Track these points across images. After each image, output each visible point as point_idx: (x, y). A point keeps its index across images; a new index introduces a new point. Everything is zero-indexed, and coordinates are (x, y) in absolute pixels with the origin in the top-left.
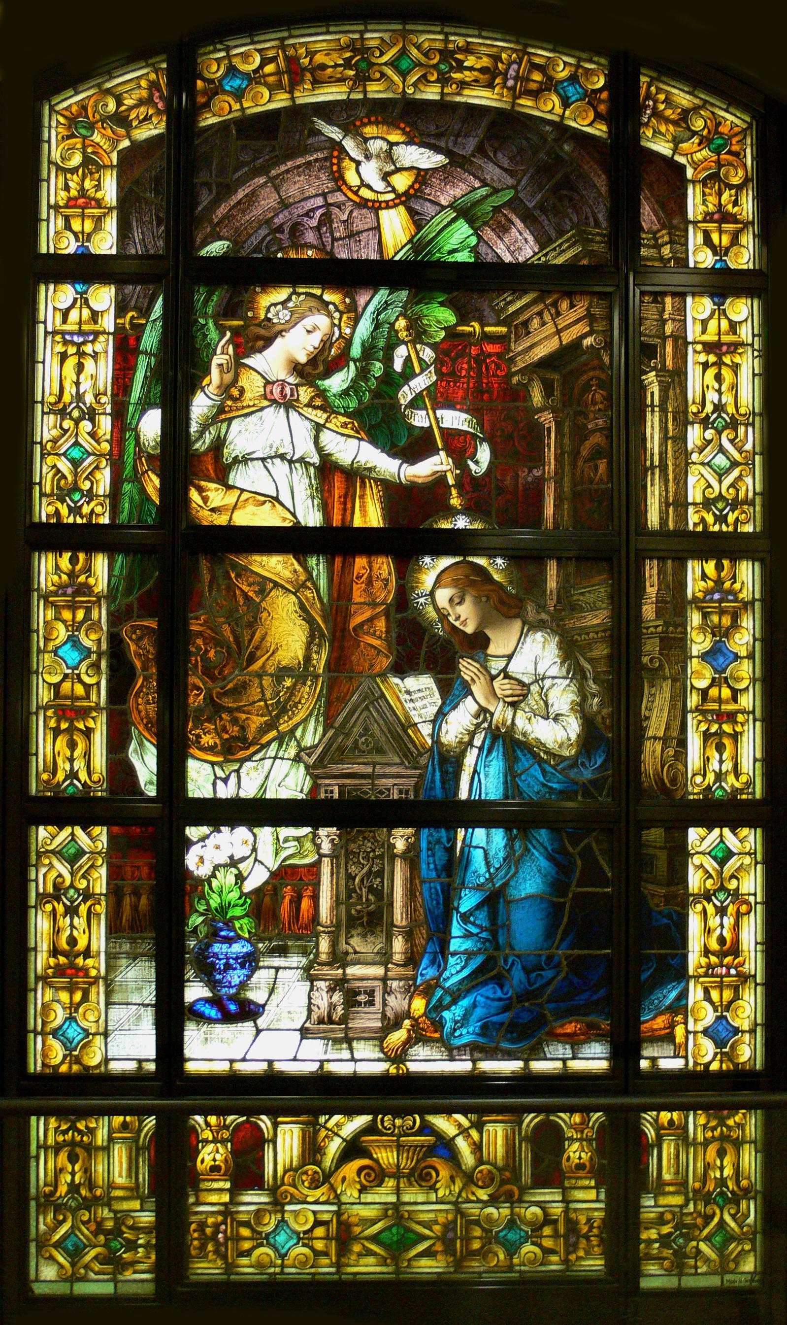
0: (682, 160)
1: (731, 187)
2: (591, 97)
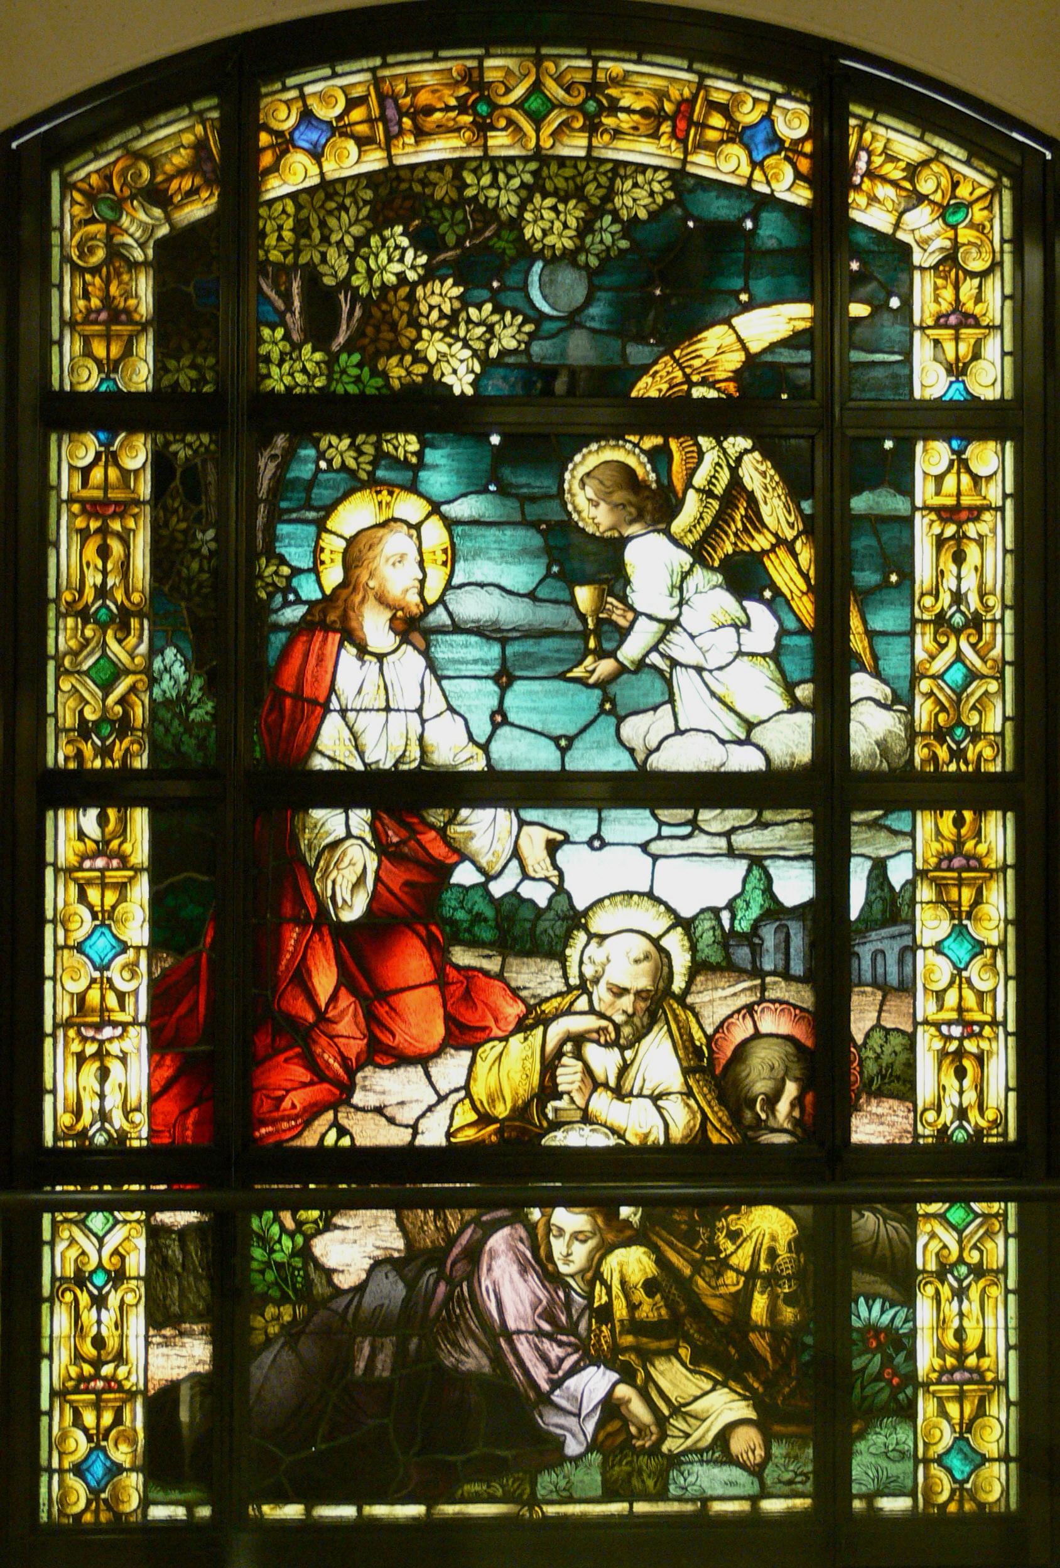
1: (973, 275)
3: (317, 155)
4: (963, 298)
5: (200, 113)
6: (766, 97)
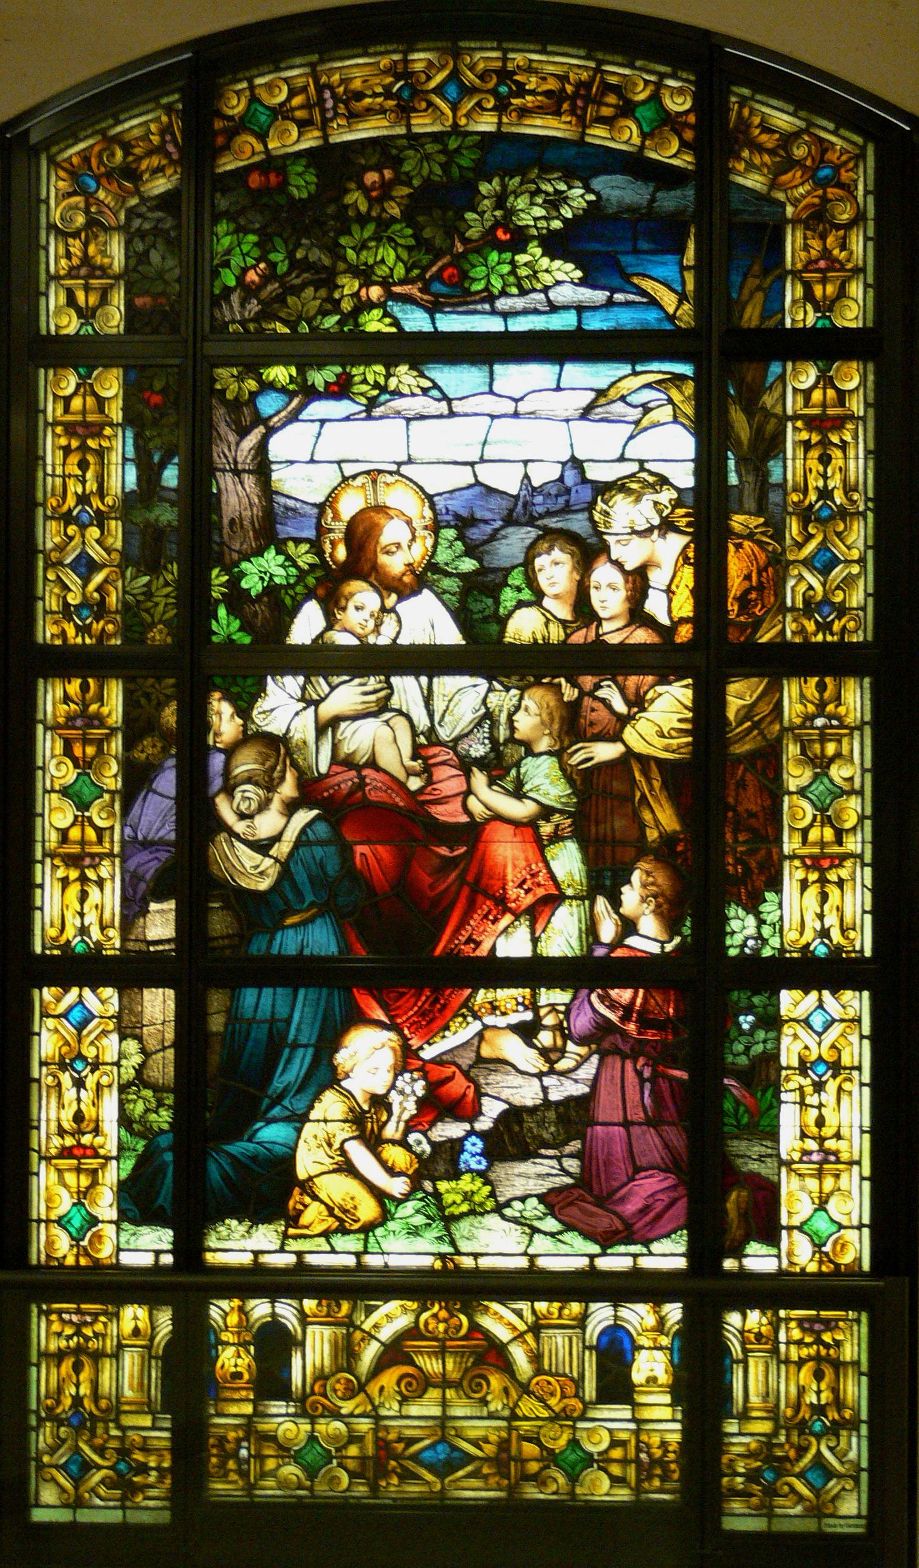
0: (780, 196)
3: (263, 137)
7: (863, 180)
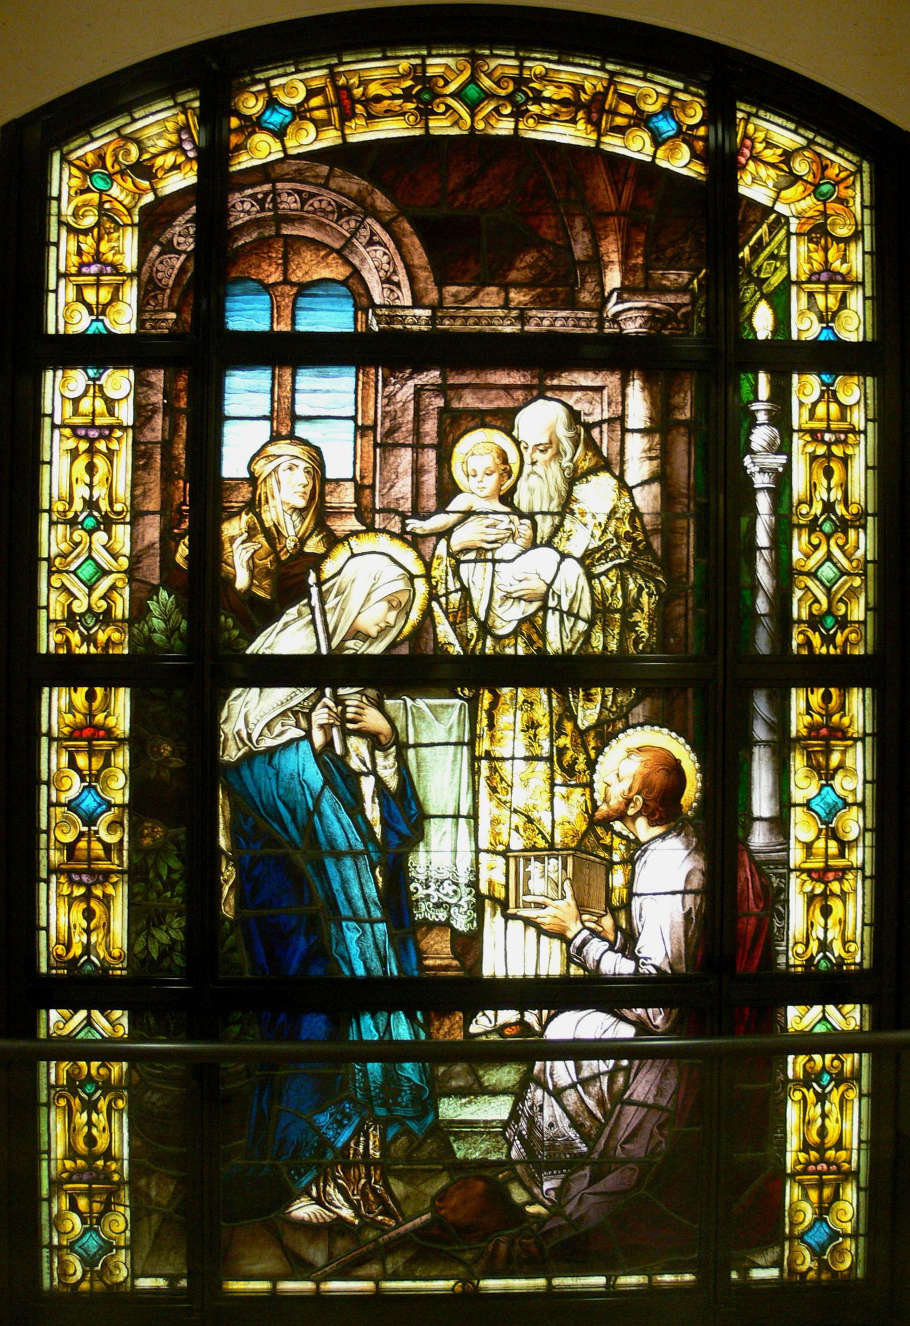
1: (839, 240)
2: (684, 135)
4: (830, 259)
5: (183, 104)
6: (666, 91)
7: (858, 196)
